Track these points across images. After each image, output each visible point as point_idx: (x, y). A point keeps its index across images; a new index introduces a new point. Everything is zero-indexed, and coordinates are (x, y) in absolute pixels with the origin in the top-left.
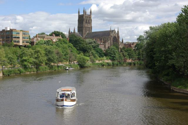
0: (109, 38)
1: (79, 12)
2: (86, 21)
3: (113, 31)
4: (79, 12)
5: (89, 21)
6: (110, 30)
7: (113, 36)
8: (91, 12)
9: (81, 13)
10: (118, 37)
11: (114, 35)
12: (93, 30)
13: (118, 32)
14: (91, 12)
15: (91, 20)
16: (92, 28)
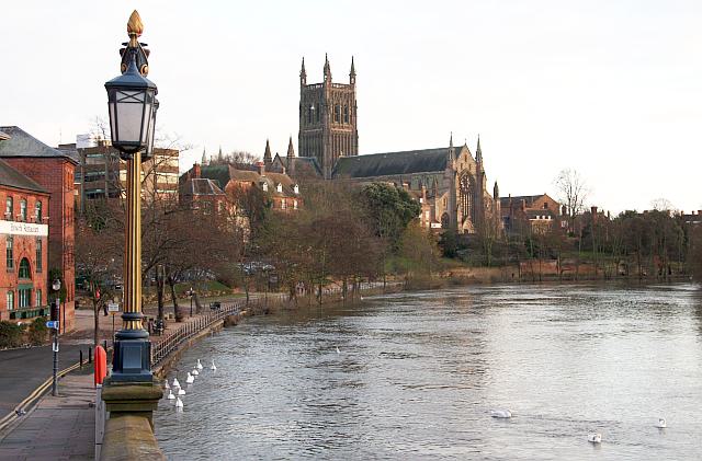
0: (445, 178)
1: (303, 75)
2: (336, 110)
3: (459, 150)
4: (303, 75)
5: (346, 111)
6: (448, 146)
7: (459, 171)
8: (352, 74)
9: (316, 77)
10: (481, 175)
11: (465, 166)
12: (366, 147)
13: (479, 153)
14: (352, 74)
15: (356, 107)
16: (357, 137)
